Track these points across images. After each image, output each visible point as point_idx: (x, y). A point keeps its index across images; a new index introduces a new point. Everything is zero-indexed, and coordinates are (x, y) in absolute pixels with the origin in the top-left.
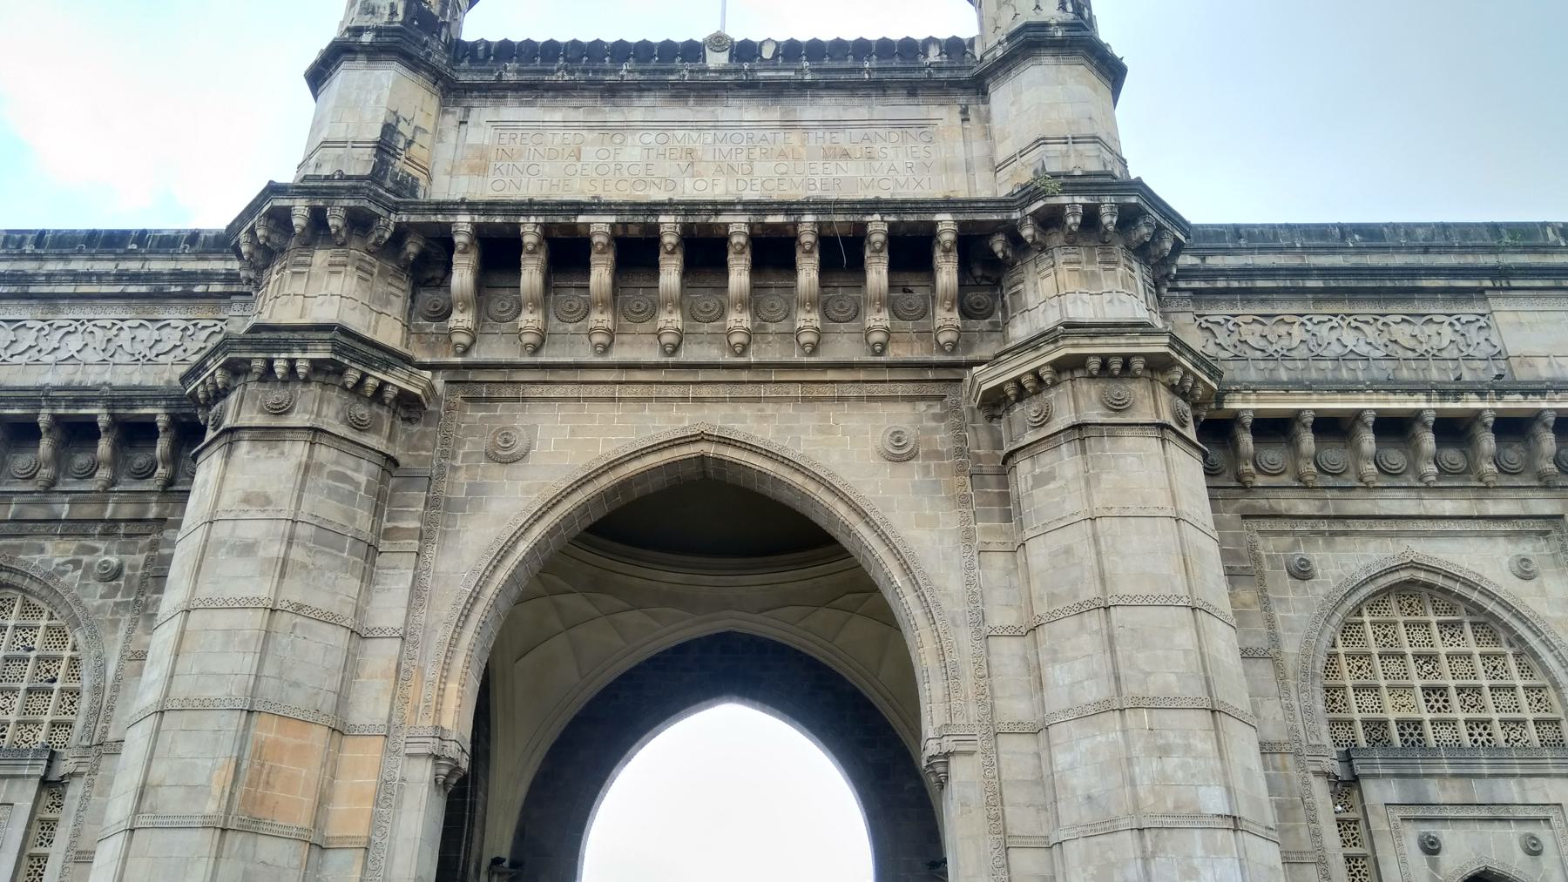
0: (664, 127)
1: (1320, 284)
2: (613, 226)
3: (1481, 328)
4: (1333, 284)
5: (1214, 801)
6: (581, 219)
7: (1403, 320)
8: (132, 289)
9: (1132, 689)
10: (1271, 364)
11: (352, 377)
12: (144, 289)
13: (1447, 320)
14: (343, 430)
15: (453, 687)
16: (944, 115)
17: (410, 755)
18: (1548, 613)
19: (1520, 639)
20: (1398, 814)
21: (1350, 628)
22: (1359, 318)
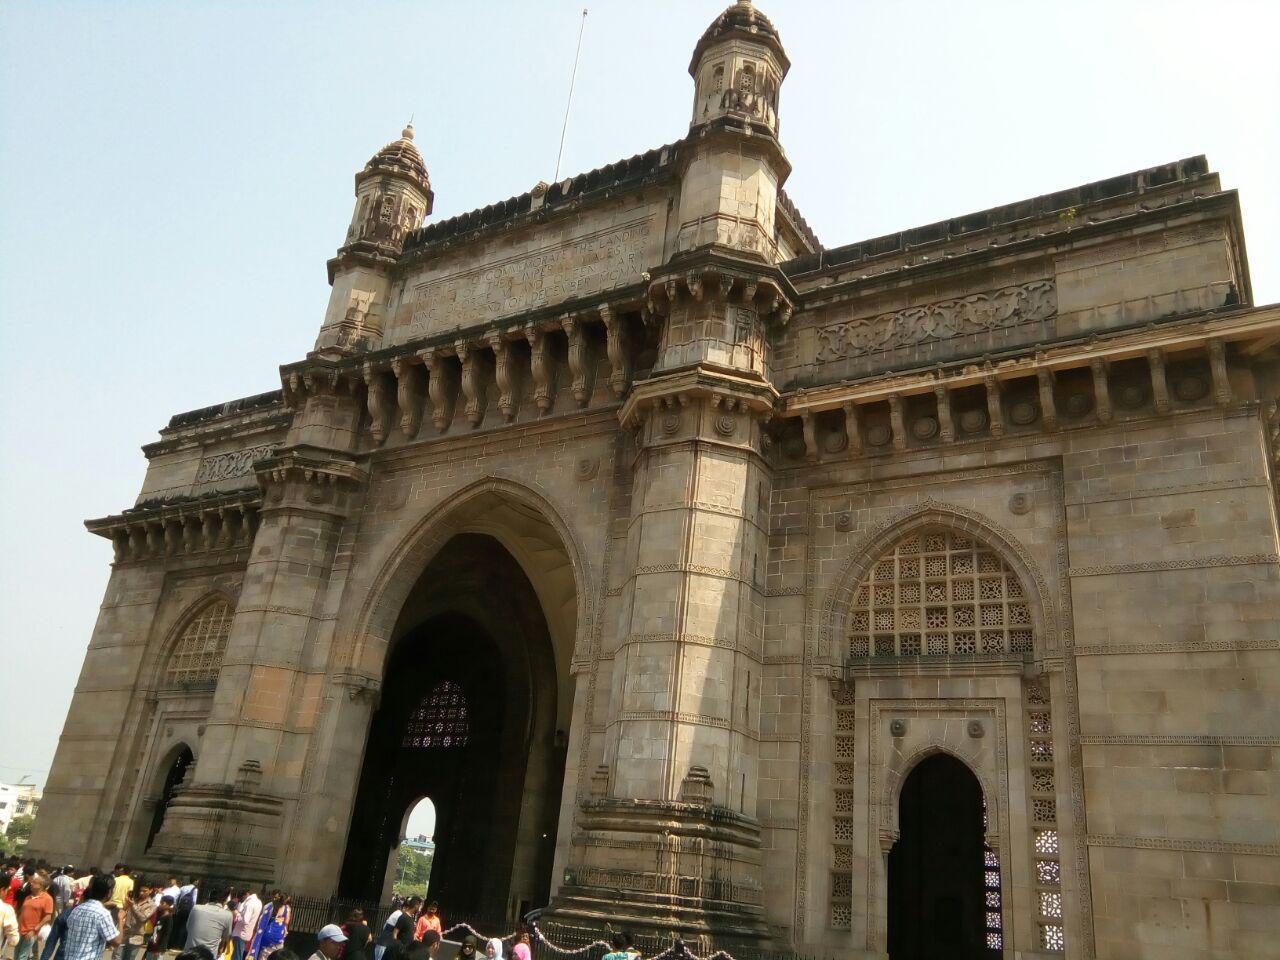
0: (499, 266)
1: (910, 283)
2: (433, 353)
3: (1045, 292)
4: (920, 280)
7: (979, 299)
8: (270, 428)
9: (636, 629)
10: (863, 360)
11: (308, 474)
12: (273, 427)
13: (1016, 290)
14: (307, 506)
15: (359, 645)
16: (656, 211)
17: (335, 684)
18: (1032, 542)
19: (1008, 568)
20: (876, 707)
22: (943, 305)
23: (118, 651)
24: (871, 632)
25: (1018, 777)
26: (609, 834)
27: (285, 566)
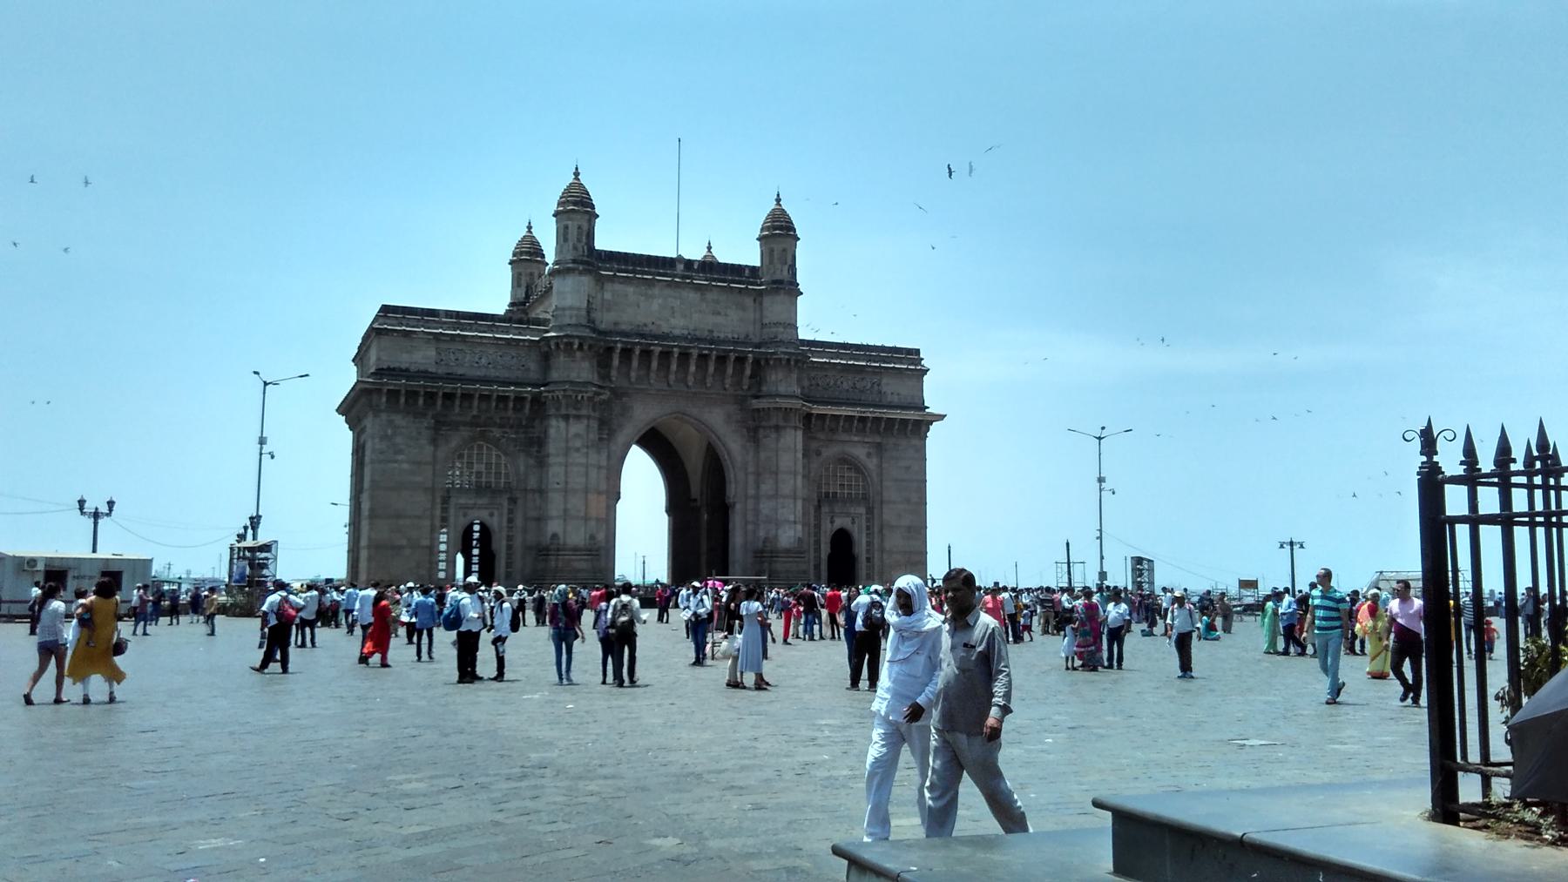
5: (793, 519)
6: (652, 348)
8: (500, 342)
14: (592, 414)
19: (863, 473)
21: (827, 469)
23: (405, 466)
24: (823, 491)
25: (864, 535)
26: (780, 559)
27: (590, 444)
